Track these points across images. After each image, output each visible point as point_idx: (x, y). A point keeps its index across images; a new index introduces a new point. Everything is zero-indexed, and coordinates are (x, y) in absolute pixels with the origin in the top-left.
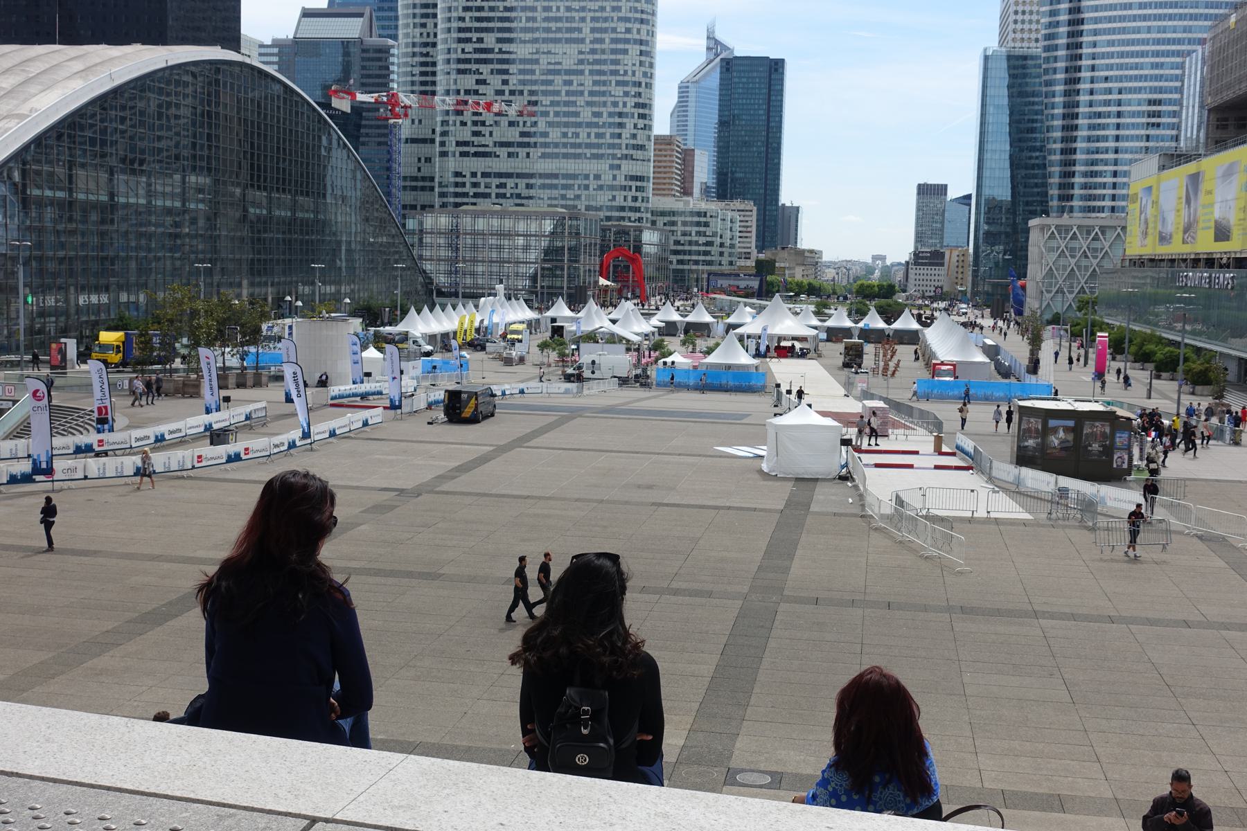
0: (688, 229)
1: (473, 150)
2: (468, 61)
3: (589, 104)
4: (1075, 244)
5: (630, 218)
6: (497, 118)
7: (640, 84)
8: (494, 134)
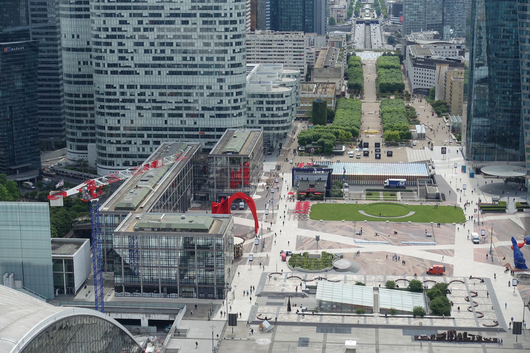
0: (270, 106)
1: (120, 70)
2: (113, 8)
3: (200, 37)
5: (233, 114)
6: (136, 48)
7: (234, 22)
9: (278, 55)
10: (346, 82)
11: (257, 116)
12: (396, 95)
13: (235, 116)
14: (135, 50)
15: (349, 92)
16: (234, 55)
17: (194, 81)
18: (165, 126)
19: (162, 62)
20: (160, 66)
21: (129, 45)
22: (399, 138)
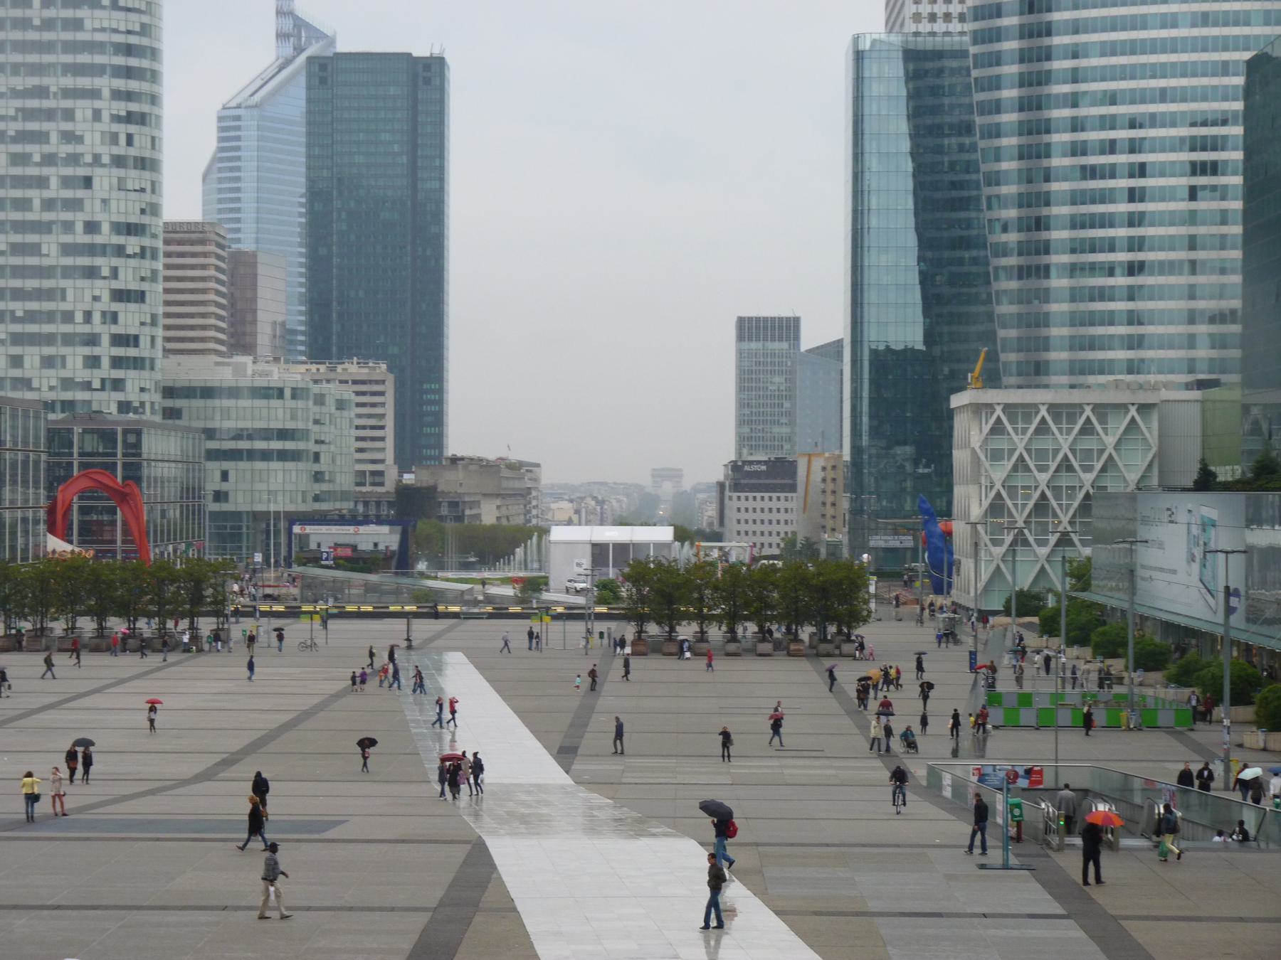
4: (1045, 443)
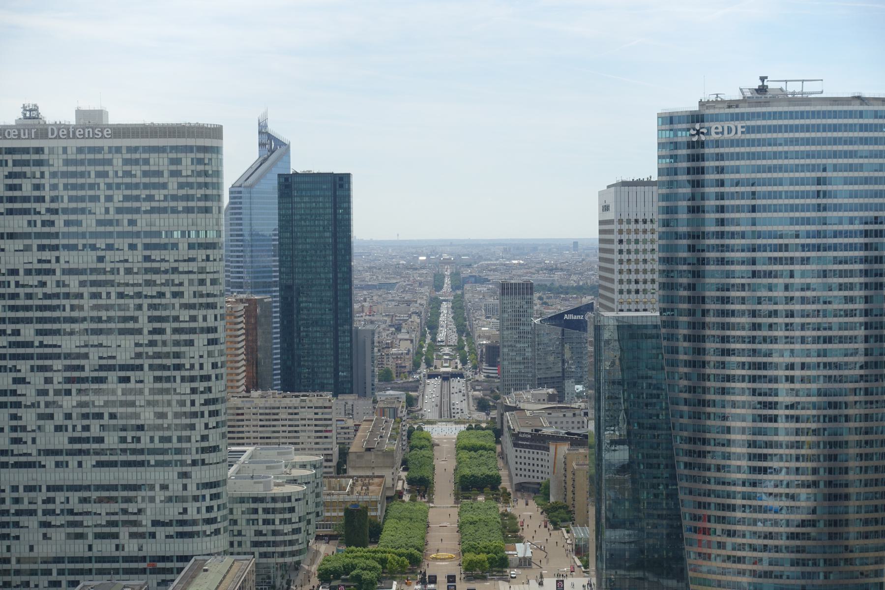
0: (270, 516)
1: (12, 460)
3: (149, 403)
5: (205, 532)
6: (41, 422)
7: (207, 378)
8: (38, 441)
9: (289, 432)
10: (404, 475)
11: (248, 535)
12: (487, 494)
13: (208, 536)
14: (39, 427)
15: (409, 491)
16: (206, 432)
17: (139, 478)
18: (90, 554)
19: (85, 446)
20: (80, 452)
21: (29, 418)
22: (487, 565)
